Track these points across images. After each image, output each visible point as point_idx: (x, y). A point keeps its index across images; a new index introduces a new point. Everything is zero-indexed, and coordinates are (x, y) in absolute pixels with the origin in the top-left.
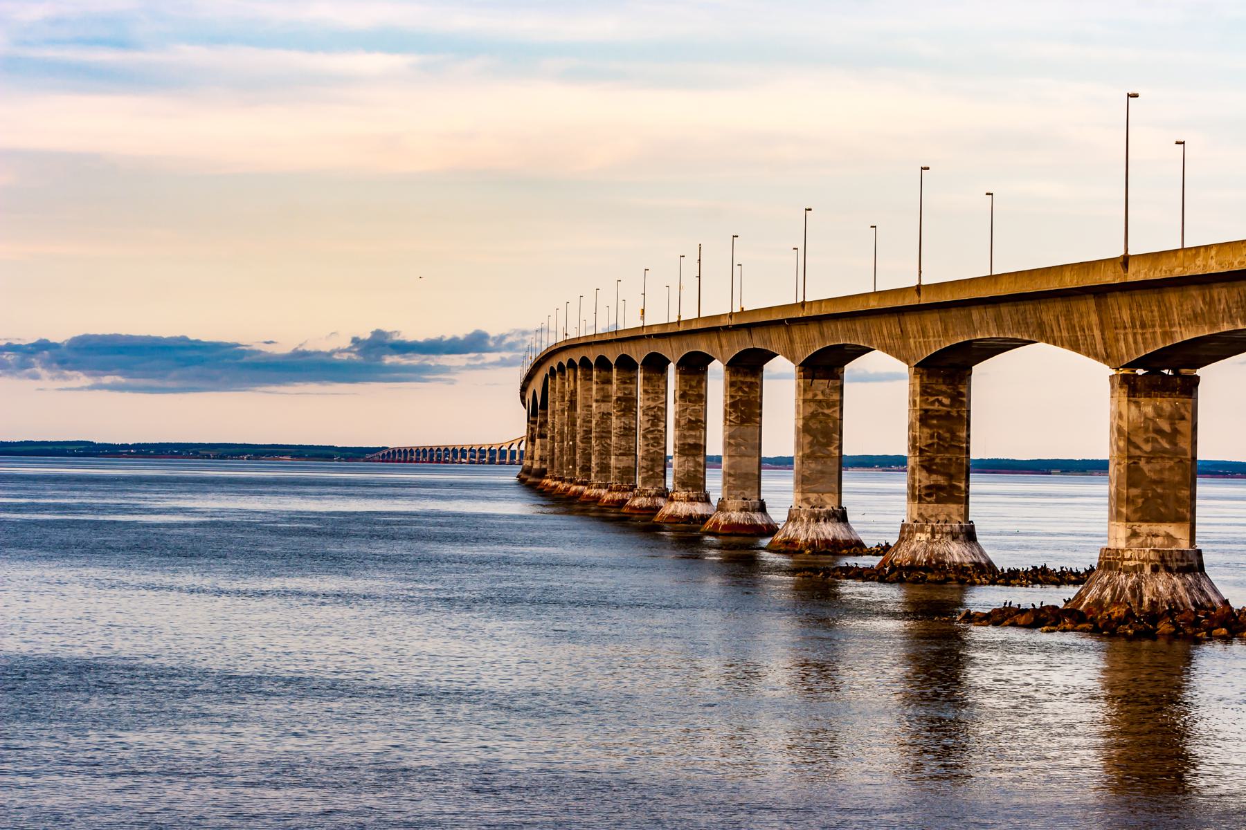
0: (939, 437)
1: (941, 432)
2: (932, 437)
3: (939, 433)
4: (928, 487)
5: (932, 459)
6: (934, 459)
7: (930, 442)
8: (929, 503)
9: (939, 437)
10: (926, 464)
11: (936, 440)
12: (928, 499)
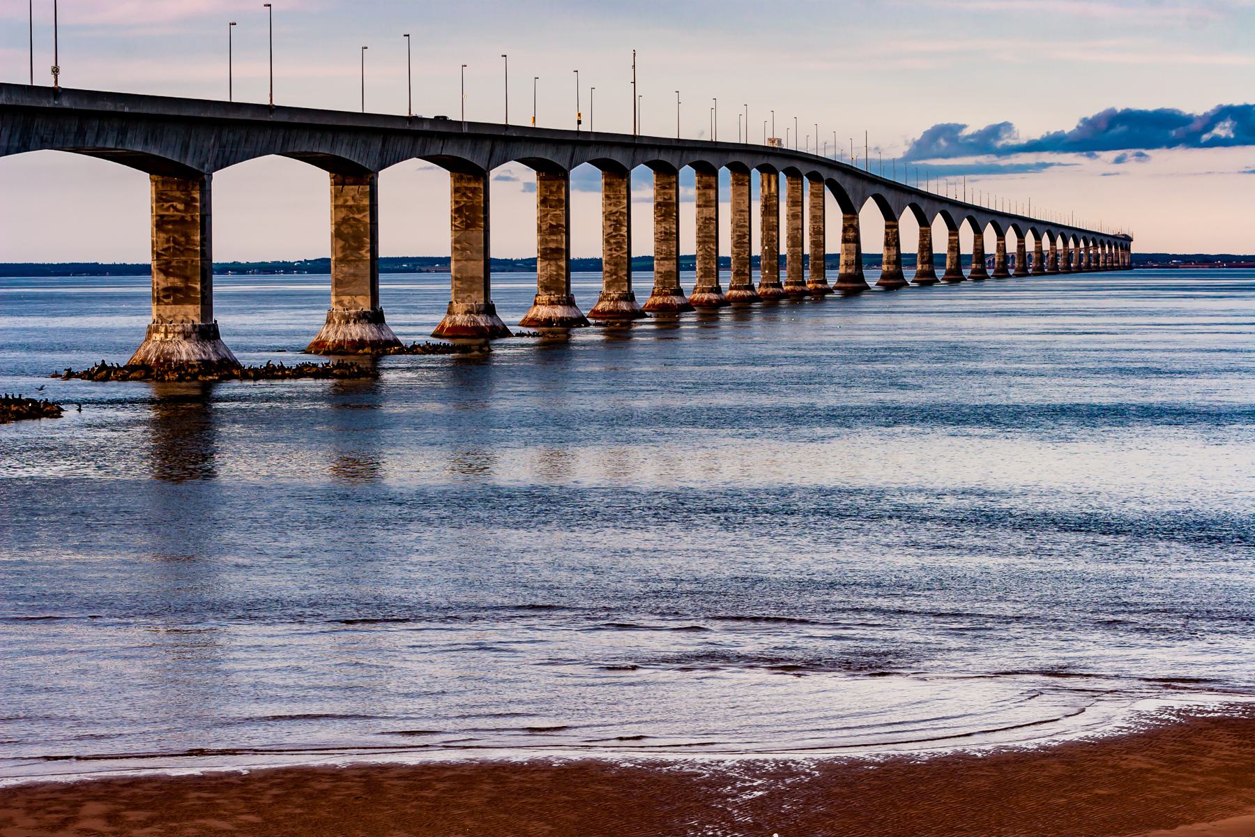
0: (175, 241)
2: (168, 241)
3: (174, 238)
4: (165, 289)
5: (168, 263)
6: (170, 262)
7: (166, 246)
8: (167, 304)
9: (175, 241)
10: (163, 267)
11: (172, 244)
12: (166, 301)
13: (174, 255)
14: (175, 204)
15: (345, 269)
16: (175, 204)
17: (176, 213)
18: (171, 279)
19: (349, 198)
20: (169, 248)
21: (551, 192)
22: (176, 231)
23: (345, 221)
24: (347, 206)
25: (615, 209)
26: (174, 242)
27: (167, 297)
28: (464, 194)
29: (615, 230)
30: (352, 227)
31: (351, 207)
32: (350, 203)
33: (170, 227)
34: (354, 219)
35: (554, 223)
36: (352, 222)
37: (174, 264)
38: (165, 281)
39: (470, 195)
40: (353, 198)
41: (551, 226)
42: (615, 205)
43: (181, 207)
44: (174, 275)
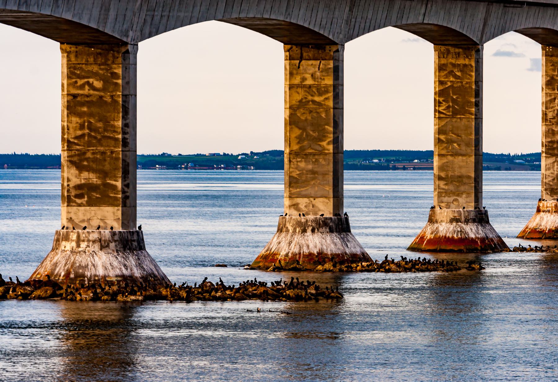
1: (92, 120)
2: (82, 127)
3: (90, 123)
5: (82, 154)
6: (85, 153)
8: (79, 205)
11: (86, 131)
12: (79, 201)
13: (89, 144)
14: (91, 80)
16: (91, 80)
17: (92, 92)
18: (85, 174)
19: (308, 76)
20: (83, 136)
22: (91, 115)
23: (302, 104)
24: (305, 86)
26: (89, 128)
28: (451, 73)
30: (311, 112)
31: (310, 87)
32: (309, 82)
33: (85, 109)
34: (314, 102)
36: (311, 106)
37: (89, 155)
38: (77, 177)
39: (459, 74)
40: (312, 75)
43: (98, 84)
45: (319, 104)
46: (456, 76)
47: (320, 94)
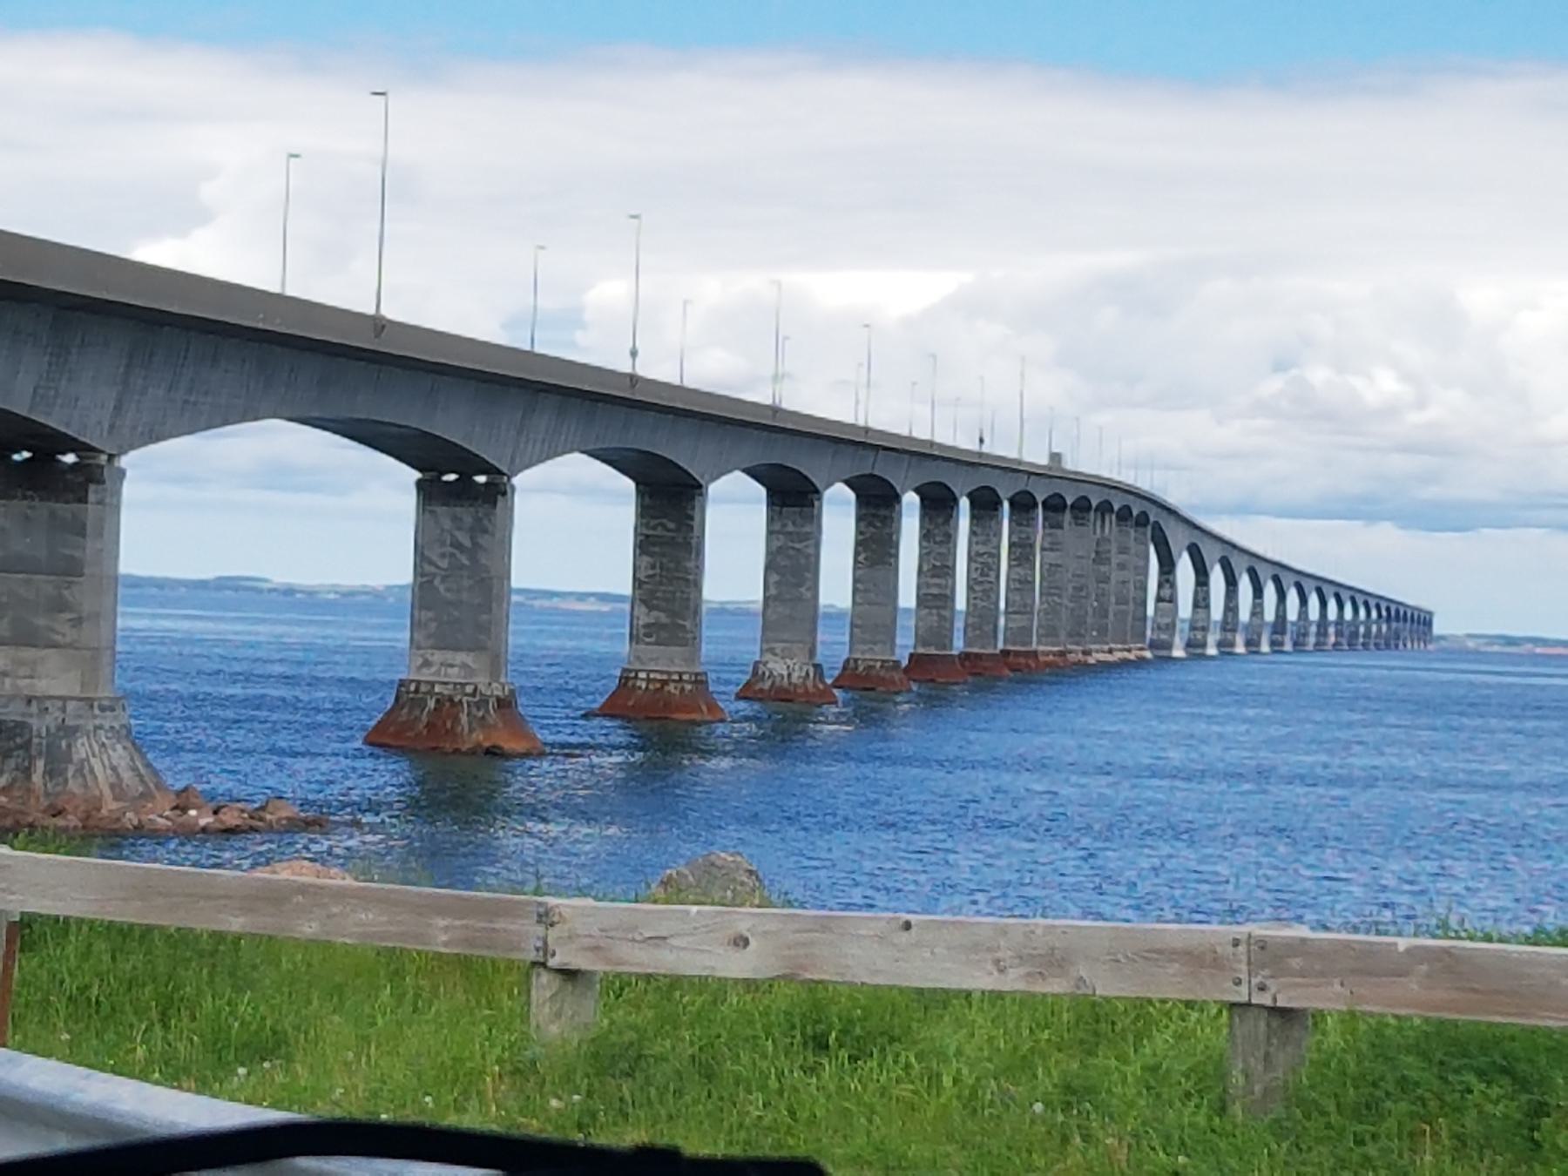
1: (665, 560)
2: (653, 567)
7: (651, 572)
11: (658, 571)
13: (661, 583)
15: (780, 609)
21: (937, 526)
22: (663, 555)
25: (982, 549)
26: (661, 568)
27: (648, 635)
29: (982, 575)
32: (790, 528)
34: (793, 548)
35: (938, 564)
36: (791, 552)
38: (648, 615)
39: (879, 524)
41: (934, 566)
42: (984, 543)
43: (671, 525)
44: (656, 608)
45: (798, 550)
46: (875, 527)
47: (801, 541)
